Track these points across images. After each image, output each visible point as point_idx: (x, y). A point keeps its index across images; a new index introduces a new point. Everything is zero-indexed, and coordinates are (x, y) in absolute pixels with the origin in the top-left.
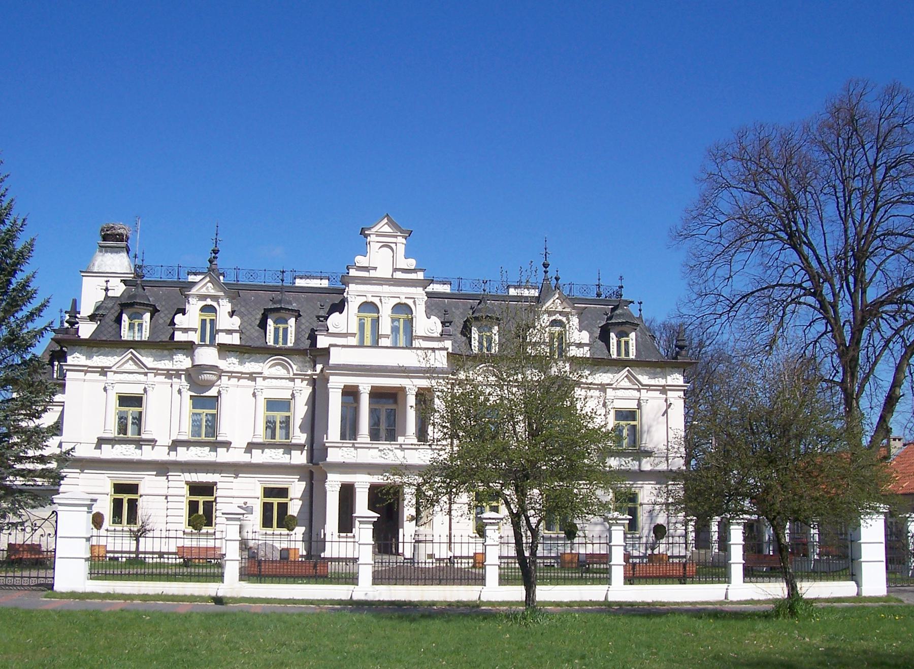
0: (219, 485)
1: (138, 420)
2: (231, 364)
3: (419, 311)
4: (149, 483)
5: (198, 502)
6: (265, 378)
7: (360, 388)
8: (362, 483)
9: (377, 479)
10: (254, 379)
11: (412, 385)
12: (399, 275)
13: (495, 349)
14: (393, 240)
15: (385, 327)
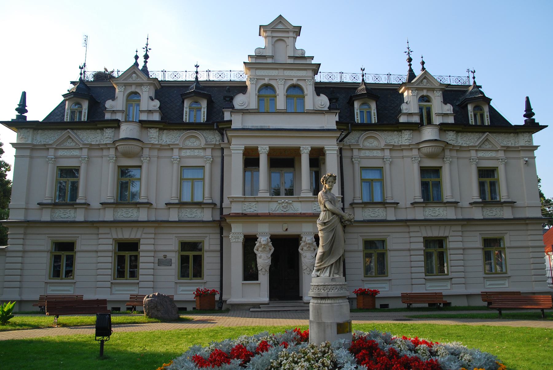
0: (142, 242)
1: (75, 188)
2: (153, 136)
3: (309, 90)
4: (84, 243)
5: (124, 256)
6: (180, 149)
8: (264, 234)
9: (279, 230)
10: (172, 149)
11: (306, 146)
13: (374, 120)
15: (281, 103)
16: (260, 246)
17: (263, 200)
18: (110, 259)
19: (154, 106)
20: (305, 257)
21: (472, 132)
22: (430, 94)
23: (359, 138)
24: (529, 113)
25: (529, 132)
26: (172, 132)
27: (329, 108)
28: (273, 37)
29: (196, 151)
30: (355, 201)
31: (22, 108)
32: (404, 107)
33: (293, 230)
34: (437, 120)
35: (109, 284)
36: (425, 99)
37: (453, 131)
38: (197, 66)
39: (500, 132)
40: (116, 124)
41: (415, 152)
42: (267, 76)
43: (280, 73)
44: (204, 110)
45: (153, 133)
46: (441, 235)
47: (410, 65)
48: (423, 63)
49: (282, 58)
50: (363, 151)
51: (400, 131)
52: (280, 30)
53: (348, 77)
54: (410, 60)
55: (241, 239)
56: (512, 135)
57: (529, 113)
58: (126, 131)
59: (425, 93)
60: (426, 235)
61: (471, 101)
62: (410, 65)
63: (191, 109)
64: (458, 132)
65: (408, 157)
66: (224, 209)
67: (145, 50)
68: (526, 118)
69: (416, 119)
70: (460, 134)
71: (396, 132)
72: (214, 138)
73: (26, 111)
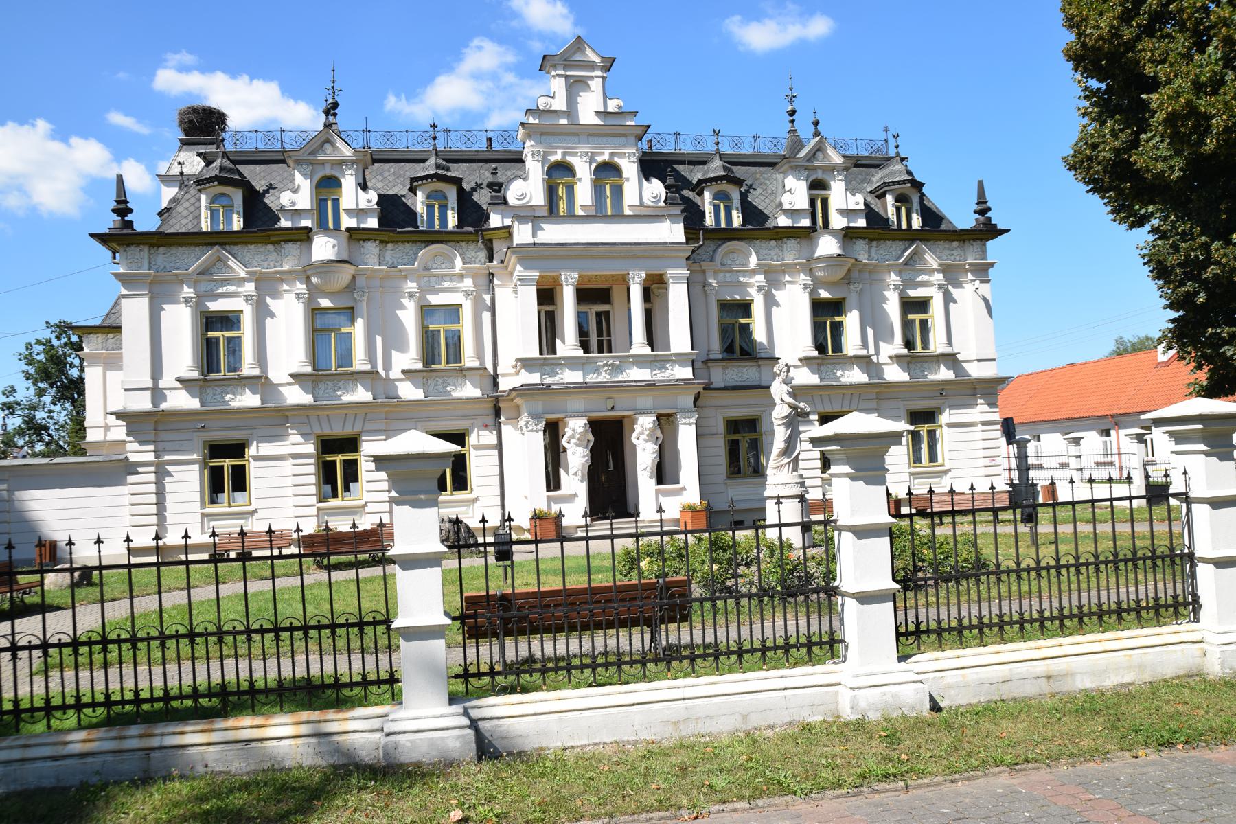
15: (584, 194)
16: (573, 437)
18: (312, 469)
19: (370, 201)
22: (826, 177)
23: (714, 251)
25: (981, 240)
26: (401, 247)
28: (566, 77)
30: (712, 357)
31: (122, 209)
34: (837, 222)
35: (314, 511)
37: (864, 238)
38: (434, 126)
39: (937, 240)
40: (303, 237)
45: (371, 249)
51: (780, 239)
53: (688, 141)
56: (955, 244)
58: (323, 248)
59: (819, 175)
60: (822, 410)
67: (331, 91)
68: (977, 216)
69: (806, 222)
70: (874, 243)
71: (773, 243)
73: (131, 211)
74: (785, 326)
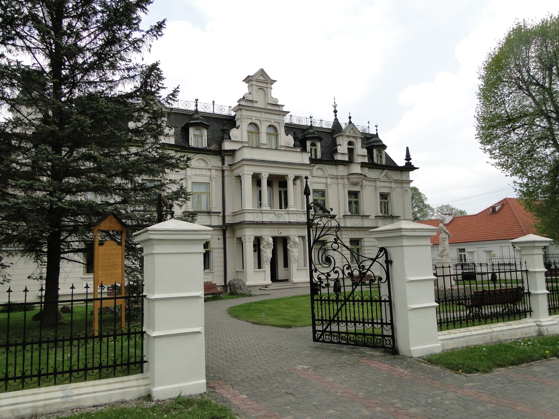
3: (282, 131)
7: (263, 175)
8: (268, 235)
9: (276, 233)
11: (291, 174)
12: (270, 107)
14: (265, 85)
17: (267, 212)
20: (266, 253)
21: (377, 169)
24: (408, 158)
27: (294, 145)
29: (204, 171)
32: (339, 148)
33: (284, 233)
36: (350, 143)
41: (346, 181)
42: (255, 116)
43: (264, 116)
44: (205, 138)
46: (360, 237)
47: (336, 115)
48: (350, 118)
49: (261, 104)
50: (314, 178)
51: (336, 165)
52: (260, 81)
54: (335, 112)
55: (252, 239)
57: (408, 158)
59: (352, 139)
60: (351, 237)
61: (376, 147)
62: (336, 115)
63: (195, 135)
64: (369, 168)
65: (341, 183)
66: (227, 218)
68: (406, 161)
69: (346, 158)
72: (214, 161)
74: (337, 202)
